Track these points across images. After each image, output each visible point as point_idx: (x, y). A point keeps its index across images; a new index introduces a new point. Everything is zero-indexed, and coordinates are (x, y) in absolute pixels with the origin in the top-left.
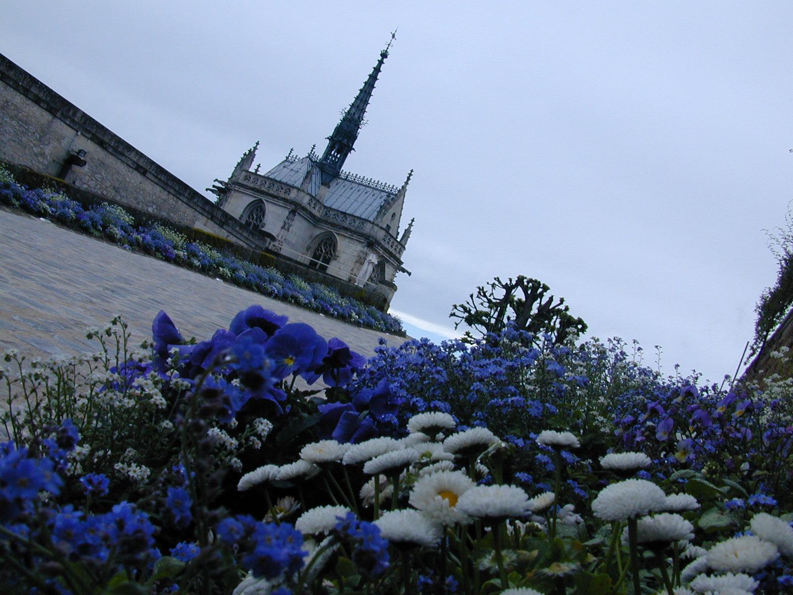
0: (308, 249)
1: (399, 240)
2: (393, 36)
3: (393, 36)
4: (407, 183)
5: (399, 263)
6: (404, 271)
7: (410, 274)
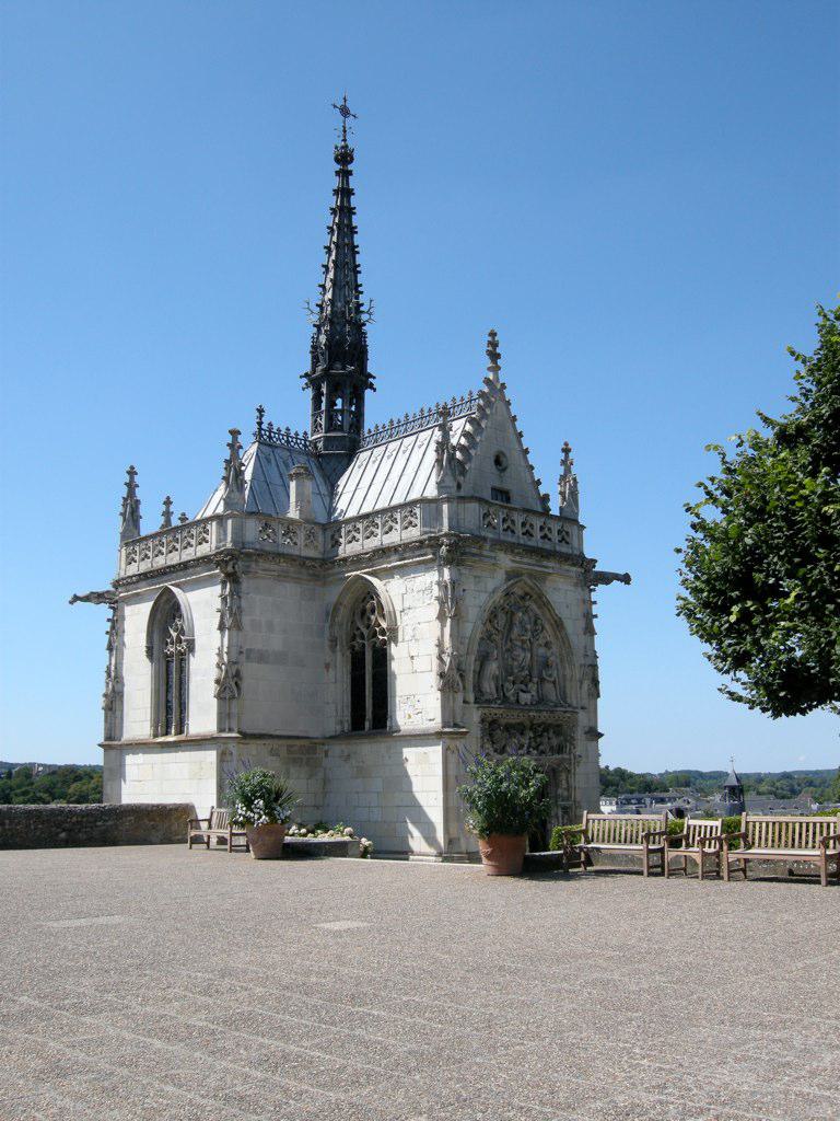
0: (334, 641)
1: (555, 511)
2: (345, 112)
3: (345, 112)
4: (496, 369)
6: (606, 578)
7: (626, 579)
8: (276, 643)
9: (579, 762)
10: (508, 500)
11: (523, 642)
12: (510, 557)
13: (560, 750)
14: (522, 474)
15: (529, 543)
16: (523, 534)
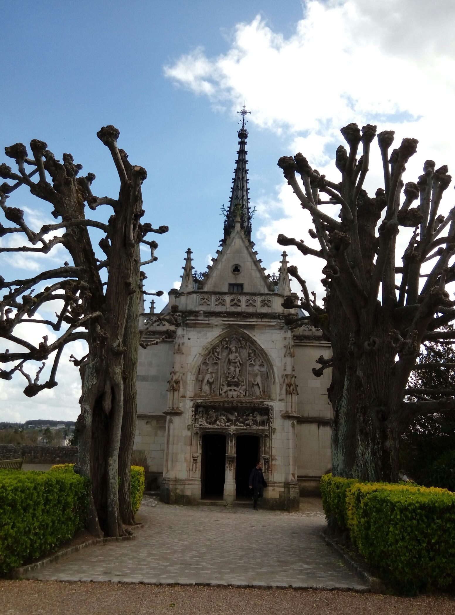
5: (280, 319)
8: (153, 372)
9: (274, 432)
10: (242, 288)
11: (235, 363)
12: (222, 319)
13: (263, 423)
14: (253, 273)
15: (236, 310)
16: (232, 306)
